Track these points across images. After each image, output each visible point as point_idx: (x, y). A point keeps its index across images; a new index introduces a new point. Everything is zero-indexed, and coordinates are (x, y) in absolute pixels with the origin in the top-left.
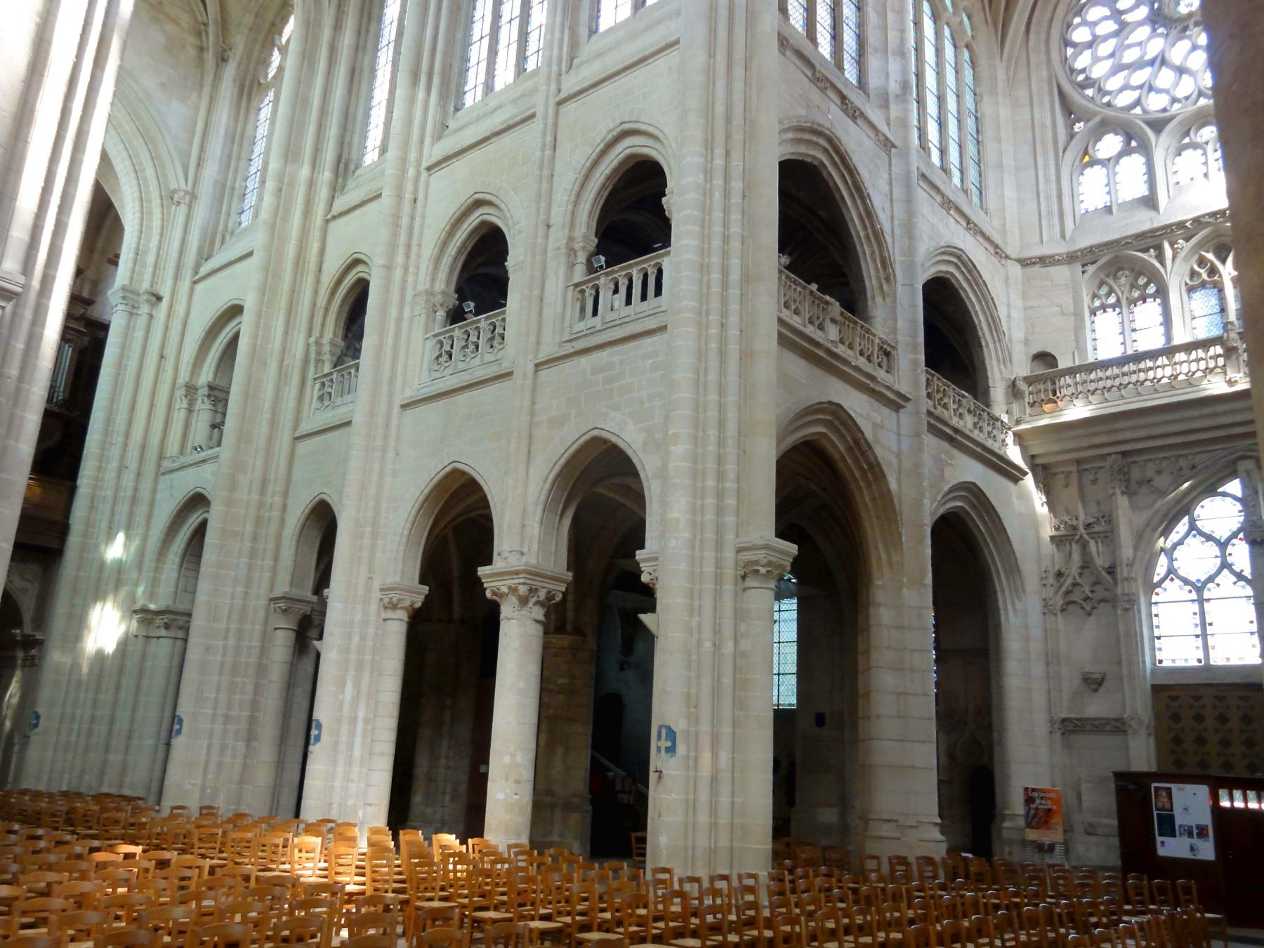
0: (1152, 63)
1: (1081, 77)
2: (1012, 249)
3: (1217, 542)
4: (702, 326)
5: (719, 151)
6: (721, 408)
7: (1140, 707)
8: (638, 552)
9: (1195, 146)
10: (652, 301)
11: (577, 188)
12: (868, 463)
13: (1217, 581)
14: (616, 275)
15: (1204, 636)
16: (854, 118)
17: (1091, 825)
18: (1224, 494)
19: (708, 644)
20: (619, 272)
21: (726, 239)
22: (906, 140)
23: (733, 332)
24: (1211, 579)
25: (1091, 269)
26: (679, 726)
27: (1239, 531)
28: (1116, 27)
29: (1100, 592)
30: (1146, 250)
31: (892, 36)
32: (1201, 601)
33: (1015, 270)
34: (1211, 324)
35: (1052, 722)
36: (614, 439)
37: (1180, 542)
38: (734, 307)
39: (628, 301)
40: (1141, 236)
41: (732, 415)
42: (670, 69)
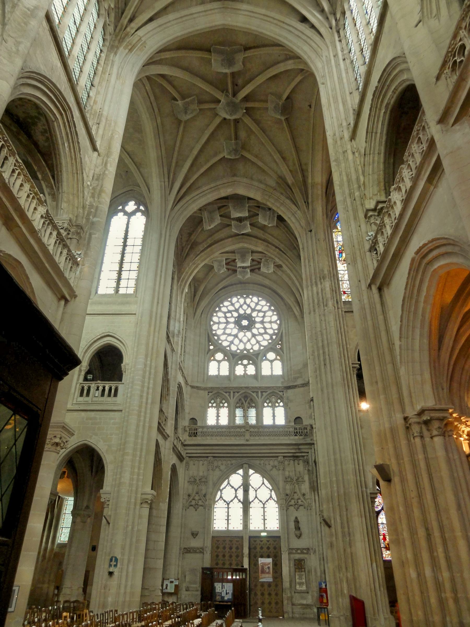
0: (234, 335)
1: (214, 332)
2: (189, 382)
3: (235, 489)
4: (139, 416)
5: (149, 359)
6: (142, 445)
7: (209, 544)
8: (101, 490)
9: (242, 364)
10: (112, 399)
11: (86, 348)
12: (159, 459)
13: (233, 501)
14: (99, 385)
15: (228, 520)
16: (168, 342)
17: (188, 587)
18: (238, 474)
19: (130, 527)
20: (101, 384)
21: (148, 388)
22: (177, 350)
23: (147, 420)
24: (232, 501)
25: (210, 394)
26: (119, 557)
27: (241, 486)
28: (225, 321)
29: (200, 503)
30: (226, 392)
31: (178, 315)
32: (228, 508)
33: (189, 388)
34: (240, 419)
35: (180, 549)
36: (93, 446)
37: (225, 488)
38: (148, 411)
39: (103, 395)
40: (226, 388)
41: (144, 447)
42: (130, 321)
